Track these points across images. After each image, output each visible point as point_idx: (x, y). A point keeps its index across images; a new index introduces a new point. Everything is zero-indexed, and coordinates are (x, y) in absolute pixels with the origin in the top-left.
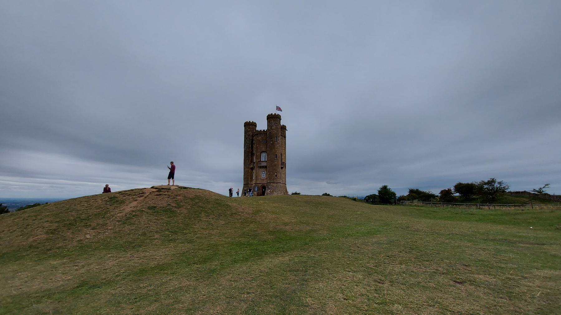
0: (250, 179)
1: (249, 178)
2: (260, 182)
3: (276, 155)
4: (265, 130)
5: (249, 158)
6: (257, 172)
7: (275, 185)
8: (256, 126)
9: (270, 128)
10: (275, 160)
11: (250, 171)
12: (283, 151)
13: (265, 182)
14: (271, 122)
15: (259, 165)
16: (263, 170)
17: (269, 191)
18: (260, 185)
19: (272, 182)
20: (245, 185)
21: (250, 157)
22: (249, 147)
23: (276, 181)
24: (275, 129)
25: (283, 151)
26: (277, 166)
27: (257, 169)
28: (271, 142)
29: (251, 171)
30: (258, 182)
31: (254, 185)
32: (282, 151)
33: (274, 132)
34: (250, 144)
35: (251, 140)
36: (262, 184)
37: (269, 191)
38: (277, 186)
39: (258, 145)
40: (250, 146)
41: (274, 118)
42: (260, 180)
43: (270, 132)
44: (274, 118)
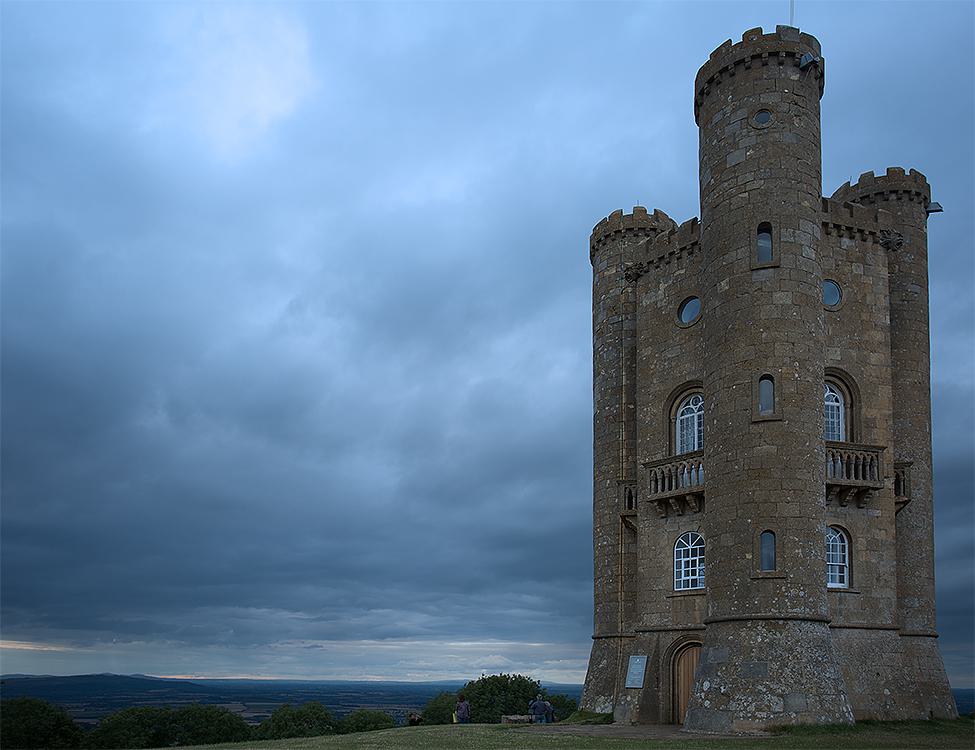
7: (759, 636)
10: (760, 428)
12: (874, 358)
17: (706, 685)
25: (874, 358)
32: (864, 361)
36: (676, 636)
37: (706, 685)
38: (771, 645)
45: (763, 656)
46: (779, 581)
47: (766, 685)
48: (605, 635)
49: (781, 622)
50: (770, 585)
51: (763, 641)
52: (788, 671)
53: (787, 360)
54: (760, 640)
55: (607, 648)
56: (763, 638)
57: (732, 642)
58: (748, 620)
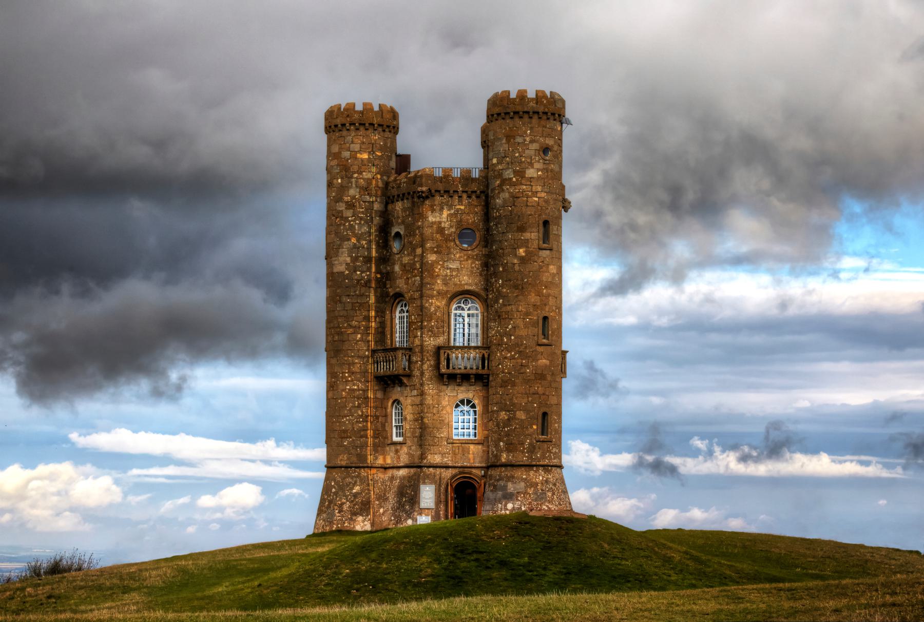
0: (375, 436)
1: (370, 433)
2: (447, 460)
3: (545, 318)
4: (476, 174)
5: (367, 319)
6: (429, 400)
8: (395, 130)
9: (516, 173)
11: (370, 395)
13: (474, 456)
14: (519, 140)
15: (443, 370)
16: (464, 393)
18: (447, 474)
19: (525, 459)
20: (330, 469)
21: (373, 313)
22: (368, 260)
23: (543, 457)
24: (539, 177)
26: (549, 378)
27: (430, 389)
28: (522, 252)
29: (380, 395)
30: (437, 459)
31: (402, 472)
33: (535, 193)
34: (370, 242)
35: (377, 220)
36: (457, 470)
38: (547, 481)
39: (432, 258)
40: (369, 249)
41: (535, 119)
42: (446, 448)
43: (515, 197)
44: (535, 119)
45: (544, 488)
46: (549, 443)
47: (547, 505)
48: (354, 465)
49: (550, 468)
50: (545, 446)
51: (543, 479)
52: (555, 497)
53: (554, 308)
54: (541, 478)
55: (357, 476)
56: (543, 477)
57: (526, 479)
58: (533, 466)
